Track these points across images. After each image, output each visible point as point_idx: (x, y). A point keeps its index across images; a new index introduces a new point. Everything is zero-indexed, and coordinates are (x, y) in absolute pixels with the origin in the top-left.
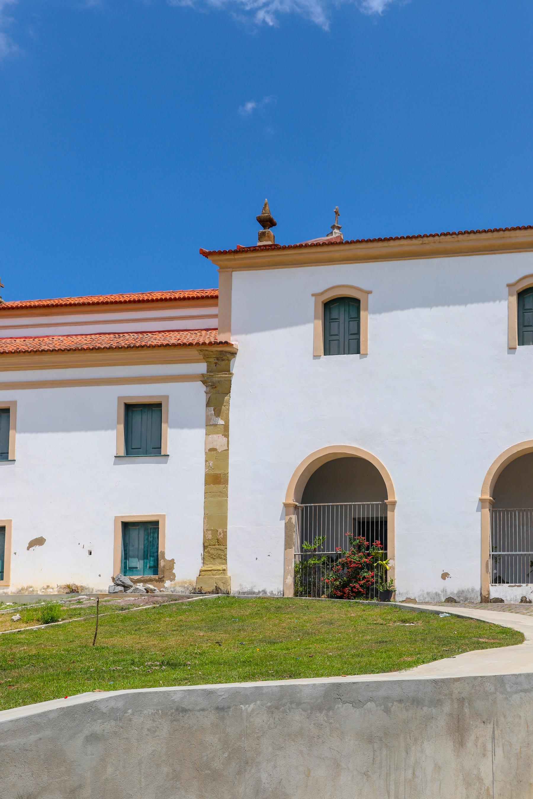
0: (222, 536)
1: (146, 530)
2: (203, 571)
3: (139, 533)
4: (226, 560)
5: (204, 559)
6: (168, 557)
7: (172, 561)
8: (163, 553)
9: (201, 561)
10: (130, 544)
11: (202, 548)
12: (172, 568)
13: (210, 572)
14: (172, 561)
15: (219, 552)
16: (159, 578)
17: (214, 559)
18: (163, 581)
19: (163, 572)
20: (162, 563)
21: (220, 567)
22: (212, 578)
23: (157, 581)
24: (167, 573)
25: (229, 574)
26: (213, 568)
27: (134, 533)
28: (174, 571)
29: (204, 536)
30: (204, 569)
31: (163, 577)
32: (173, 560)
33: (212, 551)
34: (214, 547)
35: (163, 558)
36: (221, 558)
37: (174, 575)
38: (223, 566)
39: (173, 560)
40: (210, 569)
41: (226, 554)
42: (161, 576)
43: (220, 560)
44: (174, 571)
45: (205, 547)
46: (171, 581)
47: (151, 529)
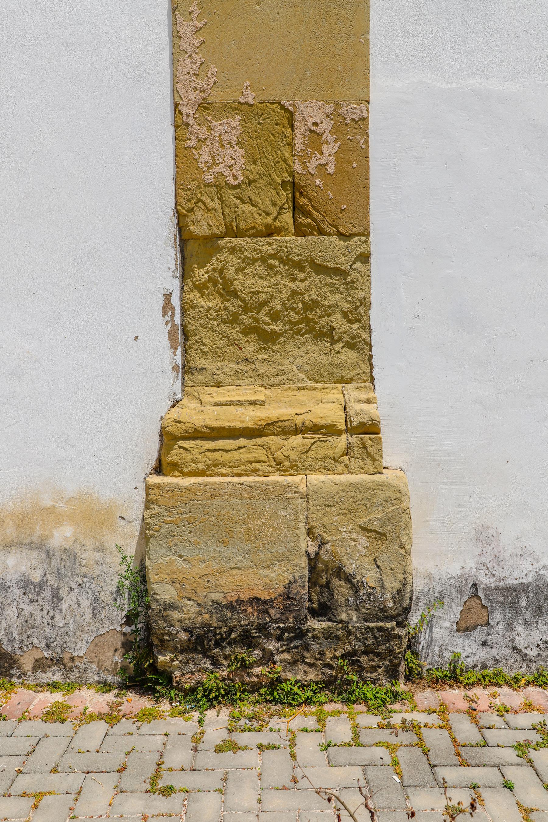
0: (328, 155)
2: (196, 435)
4: (362, 345)
5: (184, 337)
9: (161, 355)
11: (170, 256)
13: (254, 449)
15: (312, 286)
17: (267, 339)
21: (325, 406)
22: (282, 495)
25: (394, 452)
26: (273, 412)
29: (183, 158)
30: (194, 414)
33: (252, 282)
34: (263, 245)
36: (328, 334)
38: (352, 393)
40: (249, 417)
41: (365, 303)
43: (315, 352)
45: (191, 247)
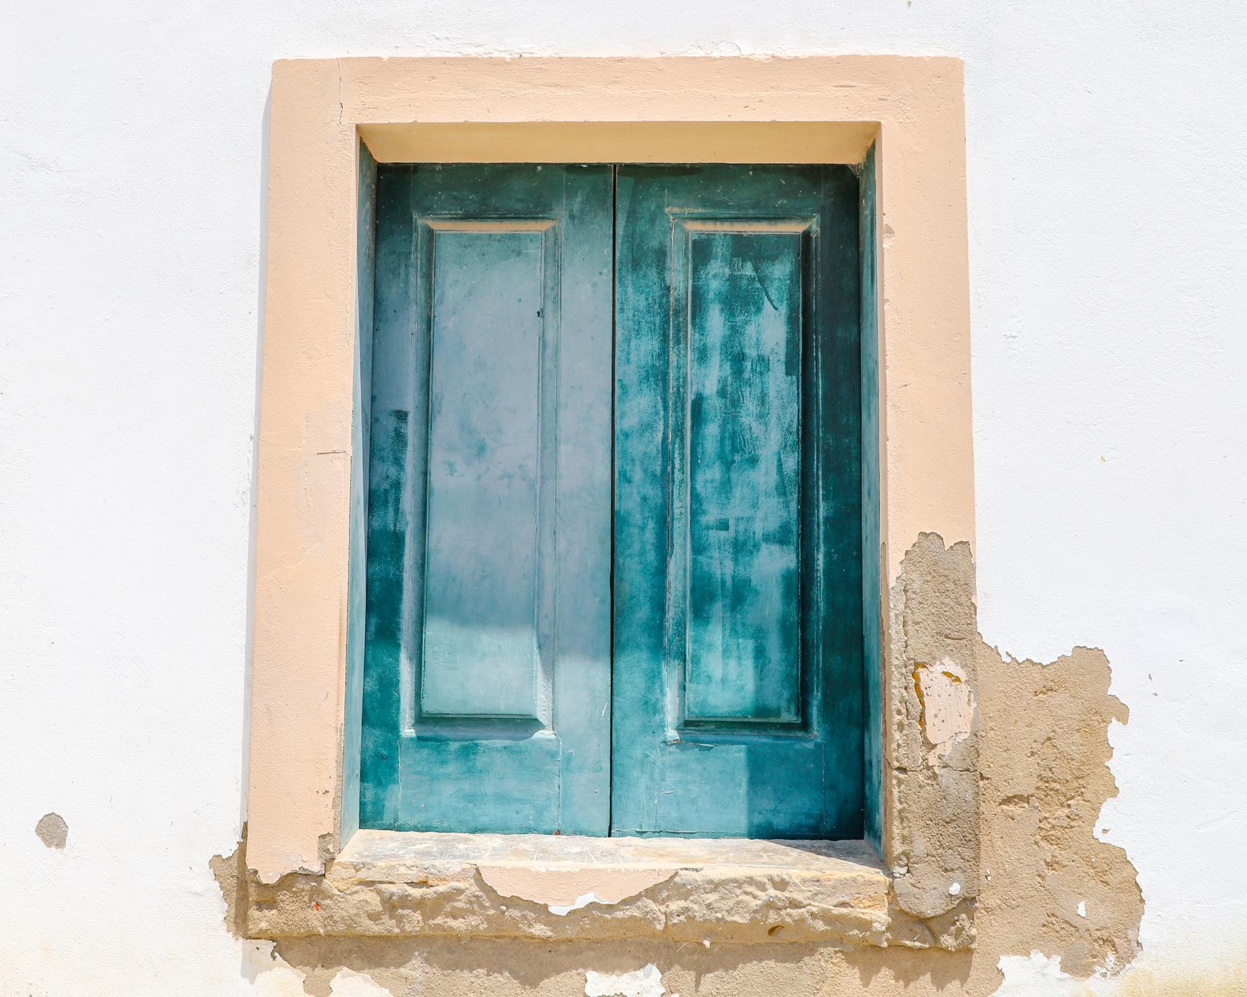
1: (636, 258)
3: (552, 293)
6: (1021, 620)
7: (1080, 691)
8: (950, 569)
10: (444, 428)
12: (1073, 780)
14: (1080, 691)
16: (910, 921)
18: (966, 951)
19: (964, 832)
20: (931, 714)
23: (866, 952)
24: (1009, 847)
27: (489, 289)
28: (1114, 824)
31: (967, 903)
32: (1090, 665)
35: (958, 631)
37: (1115, 875)
39: (1090, 665)
42: (931, 893)
44: (1114, 824)
46: (1077, 967)
47: (701, 251)
